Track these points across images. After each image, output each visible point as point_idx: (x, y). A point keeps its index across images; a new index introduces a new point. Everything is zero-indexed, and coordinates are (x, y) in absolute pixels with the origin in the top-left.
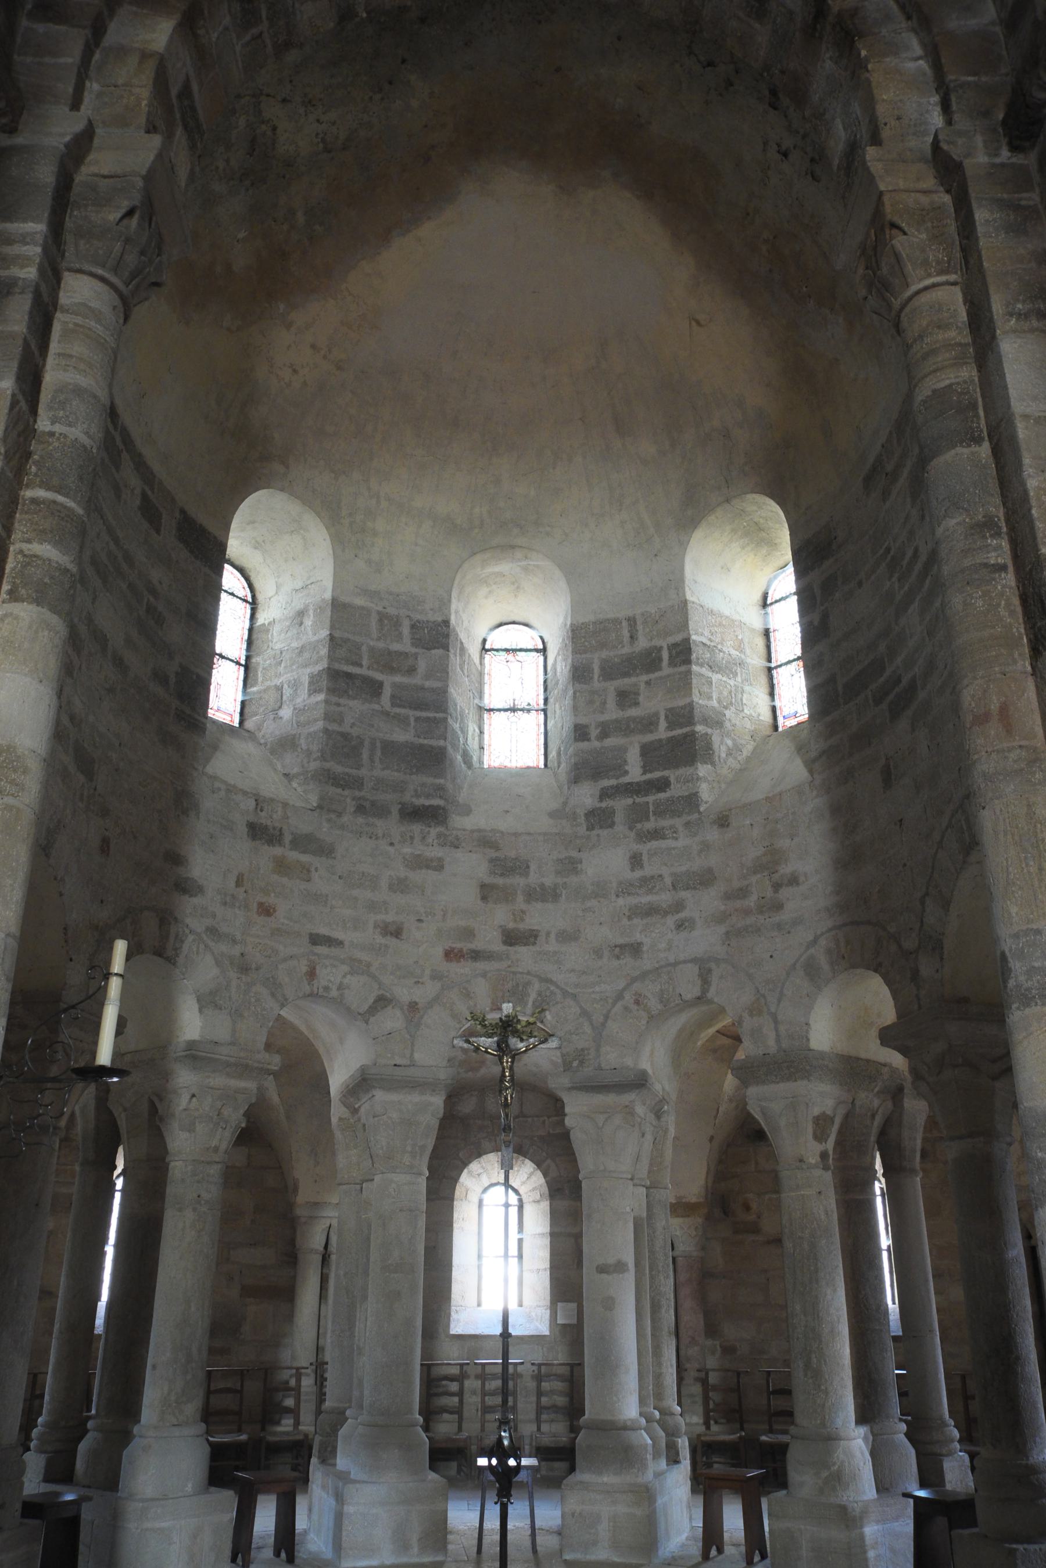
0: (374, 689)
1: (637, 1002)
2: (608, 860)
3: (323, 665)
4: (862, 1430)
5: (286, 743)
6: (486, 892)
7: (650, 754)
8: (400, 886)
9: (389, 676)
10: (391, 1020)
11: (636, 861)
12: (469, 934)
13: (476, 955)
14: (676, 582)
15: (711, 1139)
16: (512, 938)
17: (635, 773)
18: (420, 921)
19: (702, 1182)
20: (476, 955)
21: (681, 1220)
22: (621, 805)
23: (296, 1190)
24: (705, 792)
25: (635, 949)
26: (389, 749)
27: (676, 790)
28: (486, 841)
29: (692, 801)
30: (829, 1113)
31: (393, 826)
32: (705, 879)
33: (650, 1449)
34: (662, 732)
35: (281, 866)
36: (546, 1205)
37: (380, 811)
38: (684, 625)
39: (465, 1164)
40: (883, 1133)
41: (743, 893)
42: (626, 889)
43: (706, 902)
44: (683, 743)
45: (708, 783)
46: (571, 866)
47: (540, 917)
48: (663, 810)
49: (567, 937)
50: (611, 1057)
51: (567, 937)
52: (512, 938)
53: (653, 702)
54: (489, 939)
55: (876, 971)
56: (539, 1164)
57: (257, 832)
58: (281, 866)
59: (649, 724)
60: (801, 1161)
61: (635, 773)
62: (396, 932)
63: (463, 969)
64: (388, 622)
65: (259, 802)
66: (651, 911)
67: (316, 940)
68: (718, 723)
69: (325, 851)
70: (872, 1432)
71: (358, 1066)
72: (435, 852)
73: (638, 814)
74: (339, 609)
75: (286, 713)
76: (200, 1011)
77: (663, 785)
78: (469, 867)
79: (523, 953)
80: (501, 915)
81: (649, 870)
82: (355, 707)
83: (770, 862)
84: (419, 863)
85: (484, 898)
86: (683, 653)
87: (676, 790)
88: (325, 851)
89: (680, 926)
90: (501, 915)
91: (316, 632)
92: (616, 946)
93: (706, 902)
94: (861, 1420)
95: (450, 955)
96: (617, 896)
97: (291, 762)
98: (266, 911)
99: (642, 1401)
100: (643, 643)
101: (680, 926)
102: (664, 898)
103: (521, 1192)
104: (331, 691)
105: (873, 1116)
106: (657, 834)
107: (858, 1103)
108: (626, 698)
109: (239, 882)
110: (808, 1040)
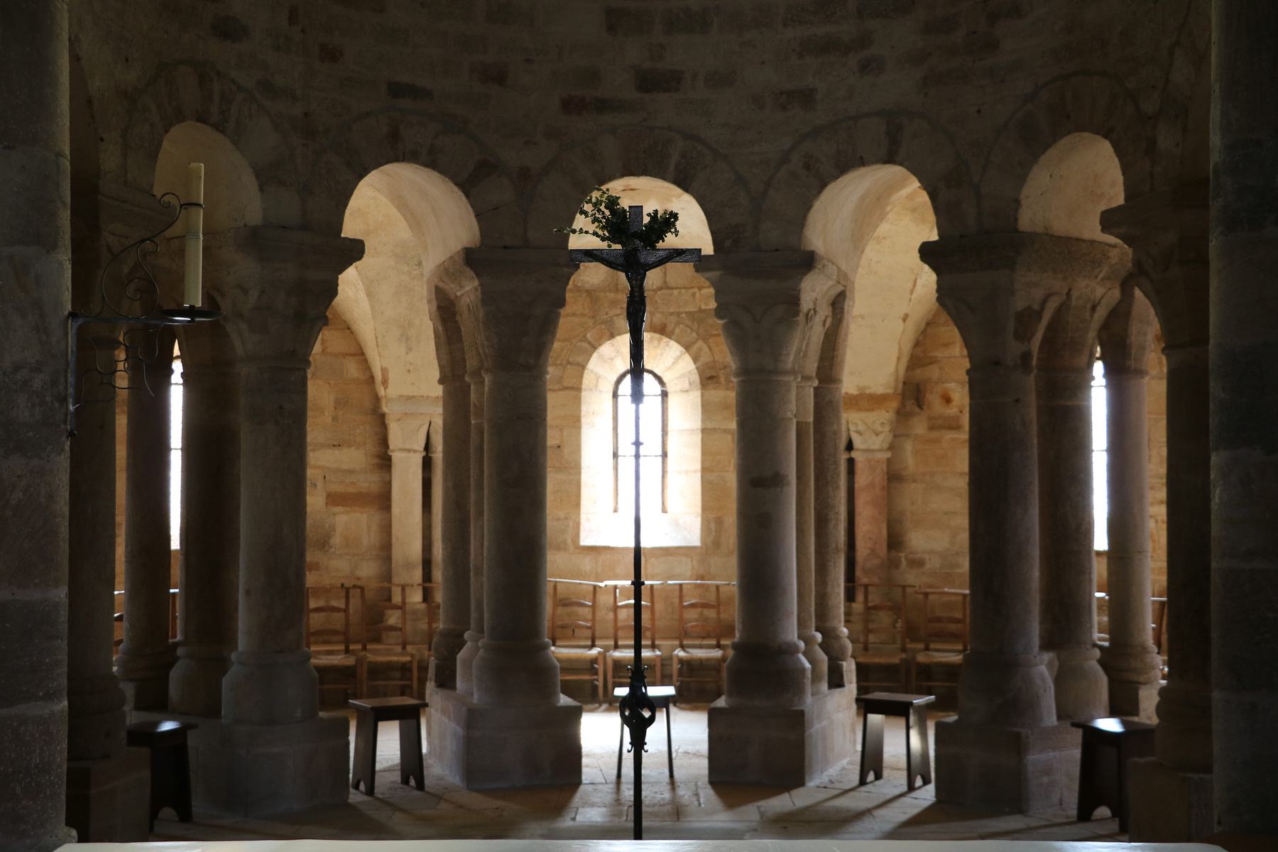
1: (807, 167)
4: (1047, 656)
13: (603, 106)
15: (905, 319)
18: (528, 61)
19: (892, 369)
20: (603, 106)
21: (863, 415)
23: (385, 382)
25: (806, 98)
30: (1036, 307)
33: (809, 674)
36: (696, 396)
39: (595, 348)
40: (1105, 327)
52: (649, 82)
55: (1106, 137)
56: (687, 347)
60: (997, 363)
67: (396, 90)
70: (1059, 659)
71: (459, 247)
76: (261, 189)
85: (611, 28)
89: (864, 67)
92: (781, 93)
94: (1047, 645)
95: (571, 106)
96: (785, 25)
98: (331, 54)
99: (802, 624)
101: (864, 67)
103: (665, 379)
105: (1094, 308)
107: (1075, 294)
109: (293, 17)
110: (1016, 220)
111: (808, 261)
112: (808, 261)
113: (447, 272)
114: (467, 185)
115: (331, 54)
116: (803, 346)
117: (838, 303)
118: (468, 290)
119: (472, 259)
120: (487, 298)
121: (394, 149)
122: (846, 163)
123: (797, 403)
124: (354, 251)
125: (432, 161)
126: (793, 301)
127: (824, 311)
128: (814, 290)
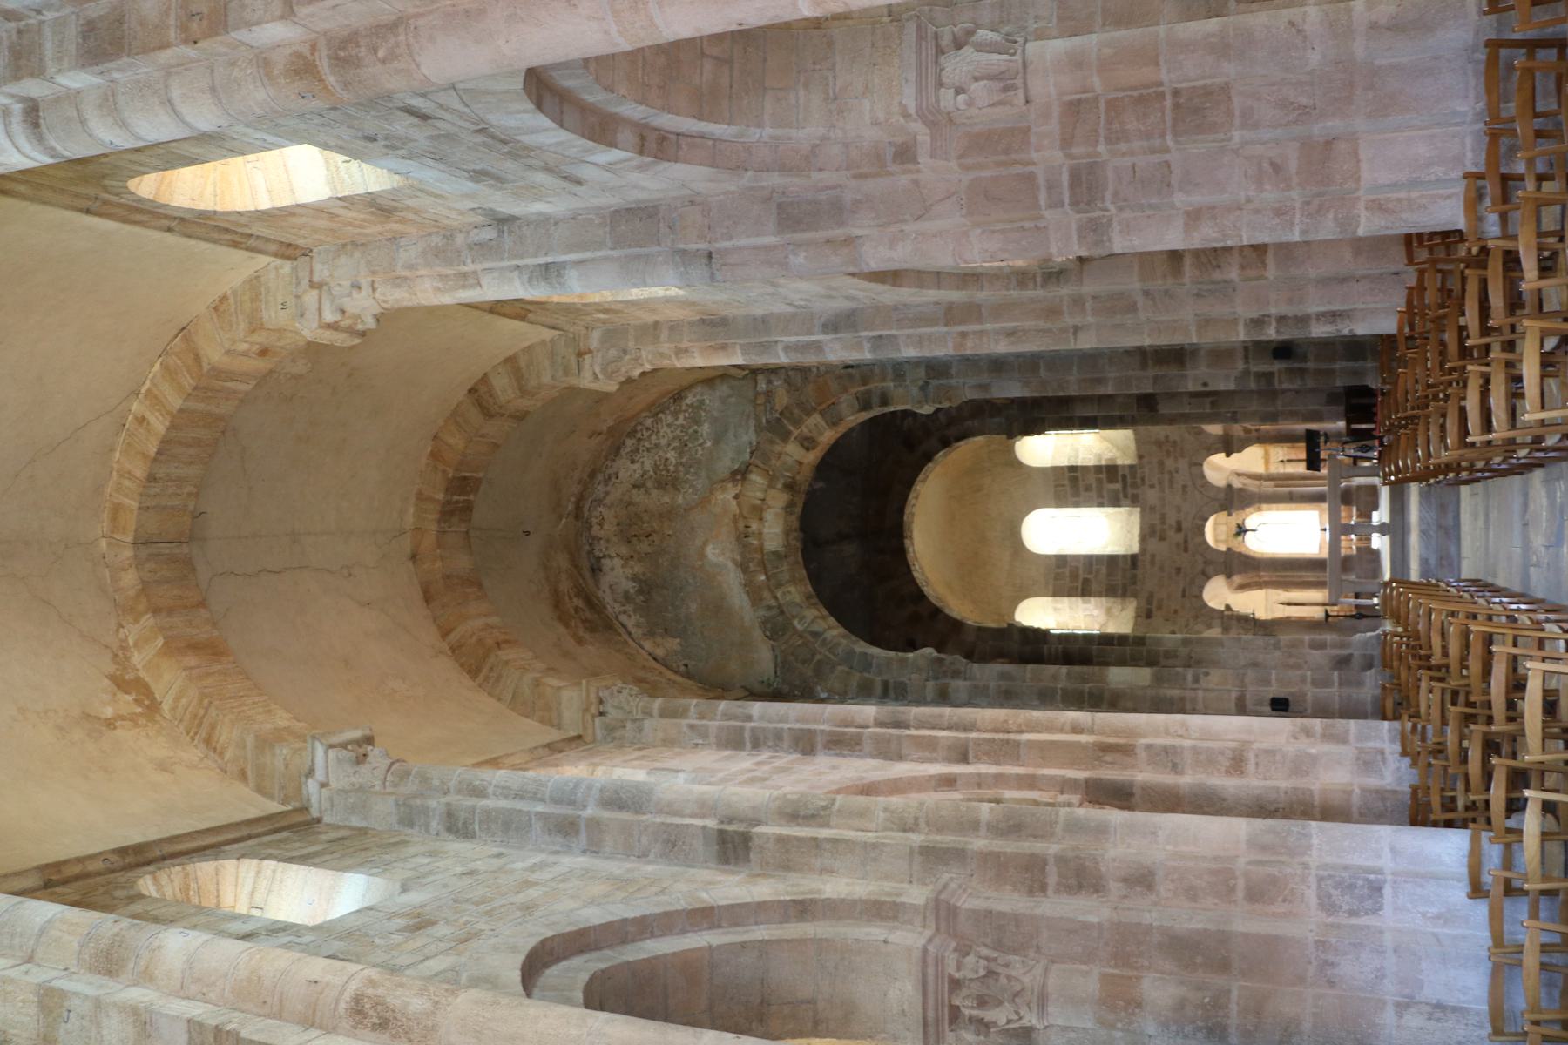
0: (1086, 581)
2: (1151, 496)
3: (1079, 600)
5: (1109, 611)
6: (1162, 538)
7: (1111, 481)
8: (1162, 569)
9: (1074, 576)
10: (1210, 569)
11: (1152, 486)
12: (1178, 545)
13: (1186, 542)
14: (1043, 471)
16: (1179, 529)
17: (1118, 486)
20: (1186, 542)
22: (1130, 491)
24: (1128, 462)
25: (1184, 487)
26: (1110, 574)
27: (1127, 472)
28: (1143, 538)
29: (1131, 467)
31: (1139, 572)
32: (1161, 464)
34: (1104, 476)
35: (1159, 608)
37: (1134, 576)
38: (1062, 468)
41: (1168, 452)
42: (1162, 490)
43: (1170, 463)
44: (1109, 471)
45: (1125, 459)
46: (1152, 509)
47: (1172, 519)
48: (1133, 475)
49: (1179, 510)
50: (1222, 495)
51: (1179, 510)
52: (1179, 529)
53: (1092, 479)
54: (1179, 537)
57: (1149, 615)
58: (1159, 608)
59: (1100, 481)
61: (1118, 486)
62: (1179, 570)
63: (1191, 546)
64: (1057, 577)
65: (1138, 616)
66: (1171, 482)
68: (1099, 456)
69: (1151, 596)
72: (1148, 557)
73: (1134, 485)
74: (1057, 593)
75: (1096, 612)
77: (1124, 477)
78: (1154, 545)
79: (1185, 525)
80: (1171, 533)
81: (1155, 481)
82: (1094, 587)
83: (1159, 444)
84: (1153, 562)
86: (1072, 469)
87: (1127, 472)
88: (1151, 596)
90: (1171, 533)
91: (1065, 602)
93: (1170, 463)
95: (1186, 550)
97: (1116, 611)
100: (1066, 482)
102: (1167, 477)
104: (1090, 595)
106: (1143, 479)
108: (1088, 488)
111: (1229, 486)
112: (1229, 486)
113: (1230, 585)
114: (1208, 578)
115: (1176, 612)
116: (1253, 486)
117: (1239, 475)
118: (1237, 579)
119: (1229, 576)
120: (1240, 573)
121: (1199, 596)
122: (1203, 477)
123: (1268, 487)
124: (1228, 607)
125: (1201, 588)
126: (1240, 490)
127: (1243, 480)
128: (1237, 484)
